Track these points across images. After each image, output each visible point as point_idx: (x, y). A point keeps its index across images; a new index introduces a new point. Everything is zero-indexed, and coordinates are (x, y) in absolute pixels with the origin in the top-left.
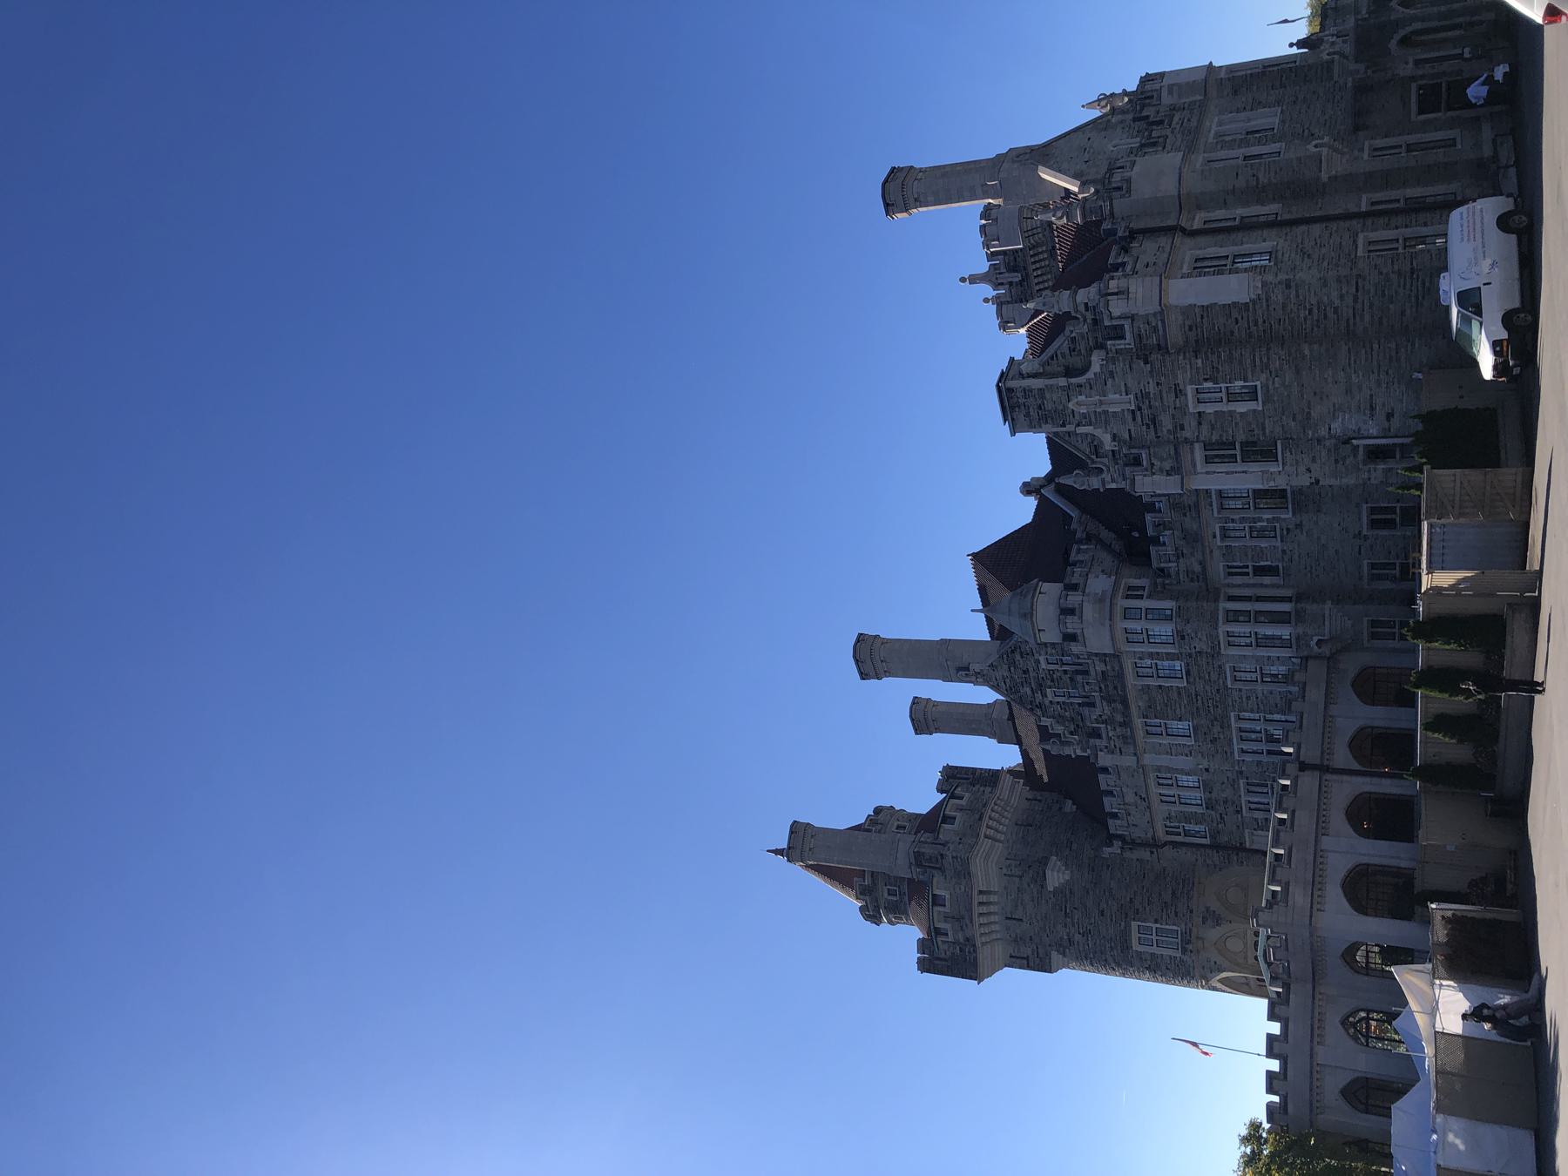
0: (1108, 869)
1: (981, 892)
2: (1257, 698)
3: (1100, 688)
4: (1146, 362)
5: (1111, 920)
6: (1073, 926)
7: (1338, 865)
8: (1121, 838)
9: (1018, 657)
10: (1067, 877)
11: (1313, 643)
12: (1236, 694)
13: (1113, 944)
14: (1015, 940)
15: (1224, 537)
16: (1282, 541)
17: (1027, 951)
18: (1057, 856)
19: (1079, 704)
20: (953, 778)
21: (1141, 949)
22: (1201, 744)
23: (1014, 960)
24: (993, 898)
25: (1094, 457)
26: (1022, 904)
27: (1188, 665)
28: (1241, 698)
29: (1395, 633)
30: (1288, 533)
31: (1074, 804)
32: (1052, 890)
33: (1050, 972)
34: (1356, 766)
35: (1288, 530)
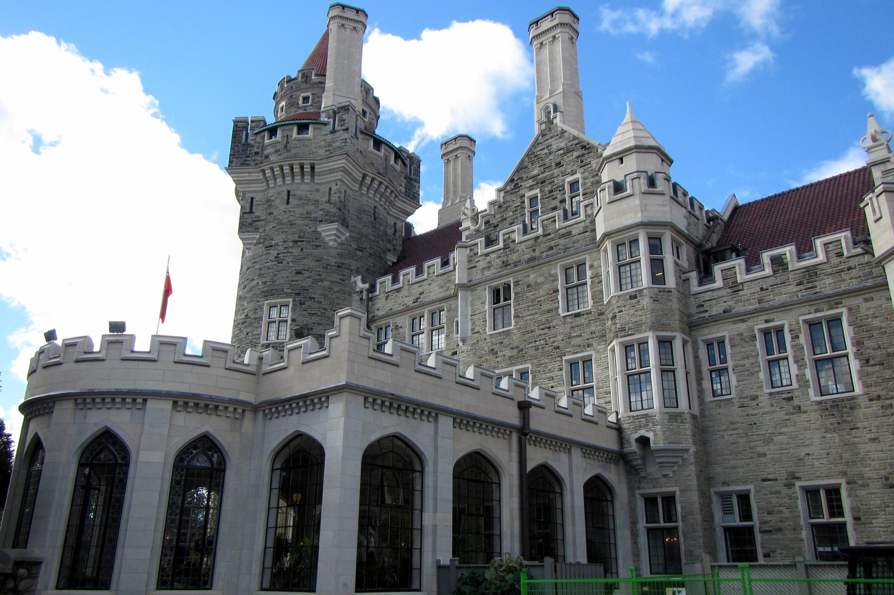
0: (340, 280)
1: (313, 168)
2: (552, 387)
3: (549, 234)
5: (292, 281)
6: (286, 248)
8: (372, 289)
9: (575, 154)
10: (331, 243)
11: (643, 432)
12: (556, 365)
13: (268, 283)
14: (268, 201)
15: (766, 333)
17: (259, 212)
18: (350, 236)
22: (488, 340)
23: (249, 200)
24: (307, 179)
26: (303, 204)
27: (587, 314)
28: (550, 371)
29: (659, 522)
30: (784, 399)
31: (394, 263)
32: (319, 229)
33: (239, 232)
35: (790, 399)
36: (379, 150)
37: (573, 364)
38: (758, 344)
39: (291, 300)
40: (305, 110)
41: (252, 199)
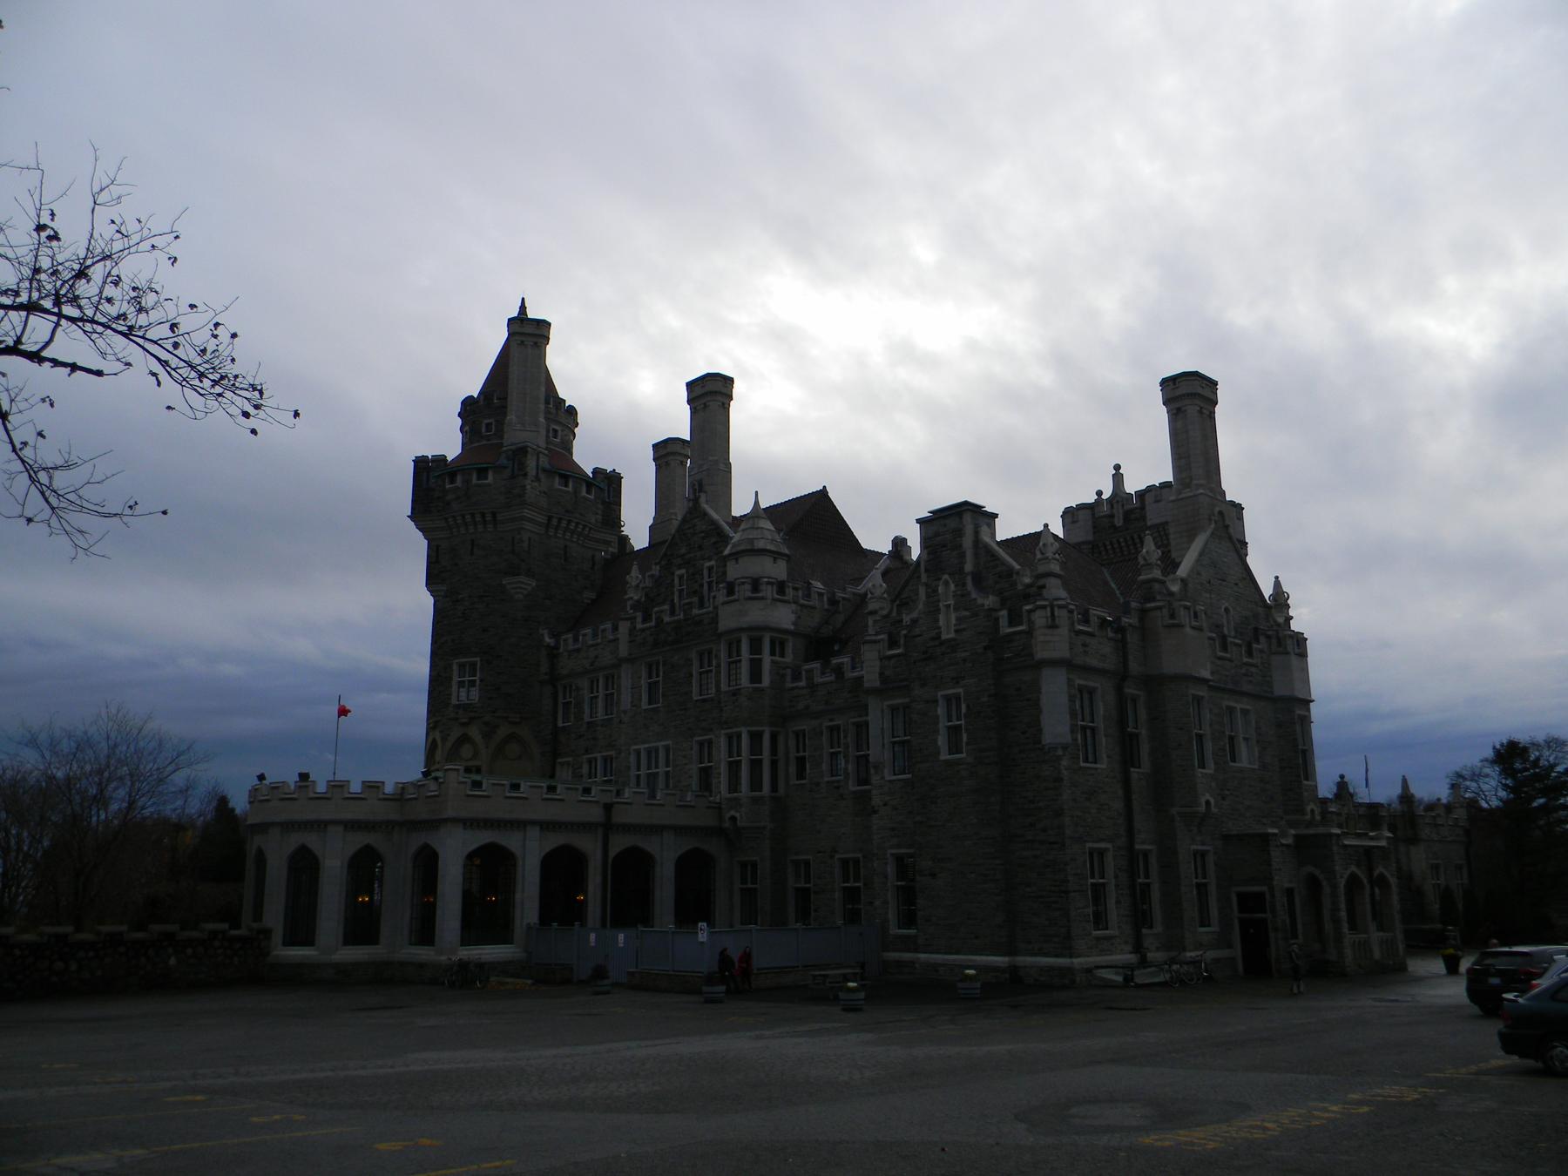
1: (494, 515)
2: (686, 764)
4: (985, 648)
7: (511, 841)
9: (713, 540)
11: (732, 813)
15: (831, 729)
16: (828, 782)
19: (673, 600)
20: (608, 484)
21: (455, 667)
24: (490, 527)
25: (898, 602)
32: (504, 582)
34: (612, 854)
35: (838, 788)
36: (566, 486)
37: (701, 744)
38: (825, 738)
39: (478, 659)
40: (489, 440)
41: (438, 547)
